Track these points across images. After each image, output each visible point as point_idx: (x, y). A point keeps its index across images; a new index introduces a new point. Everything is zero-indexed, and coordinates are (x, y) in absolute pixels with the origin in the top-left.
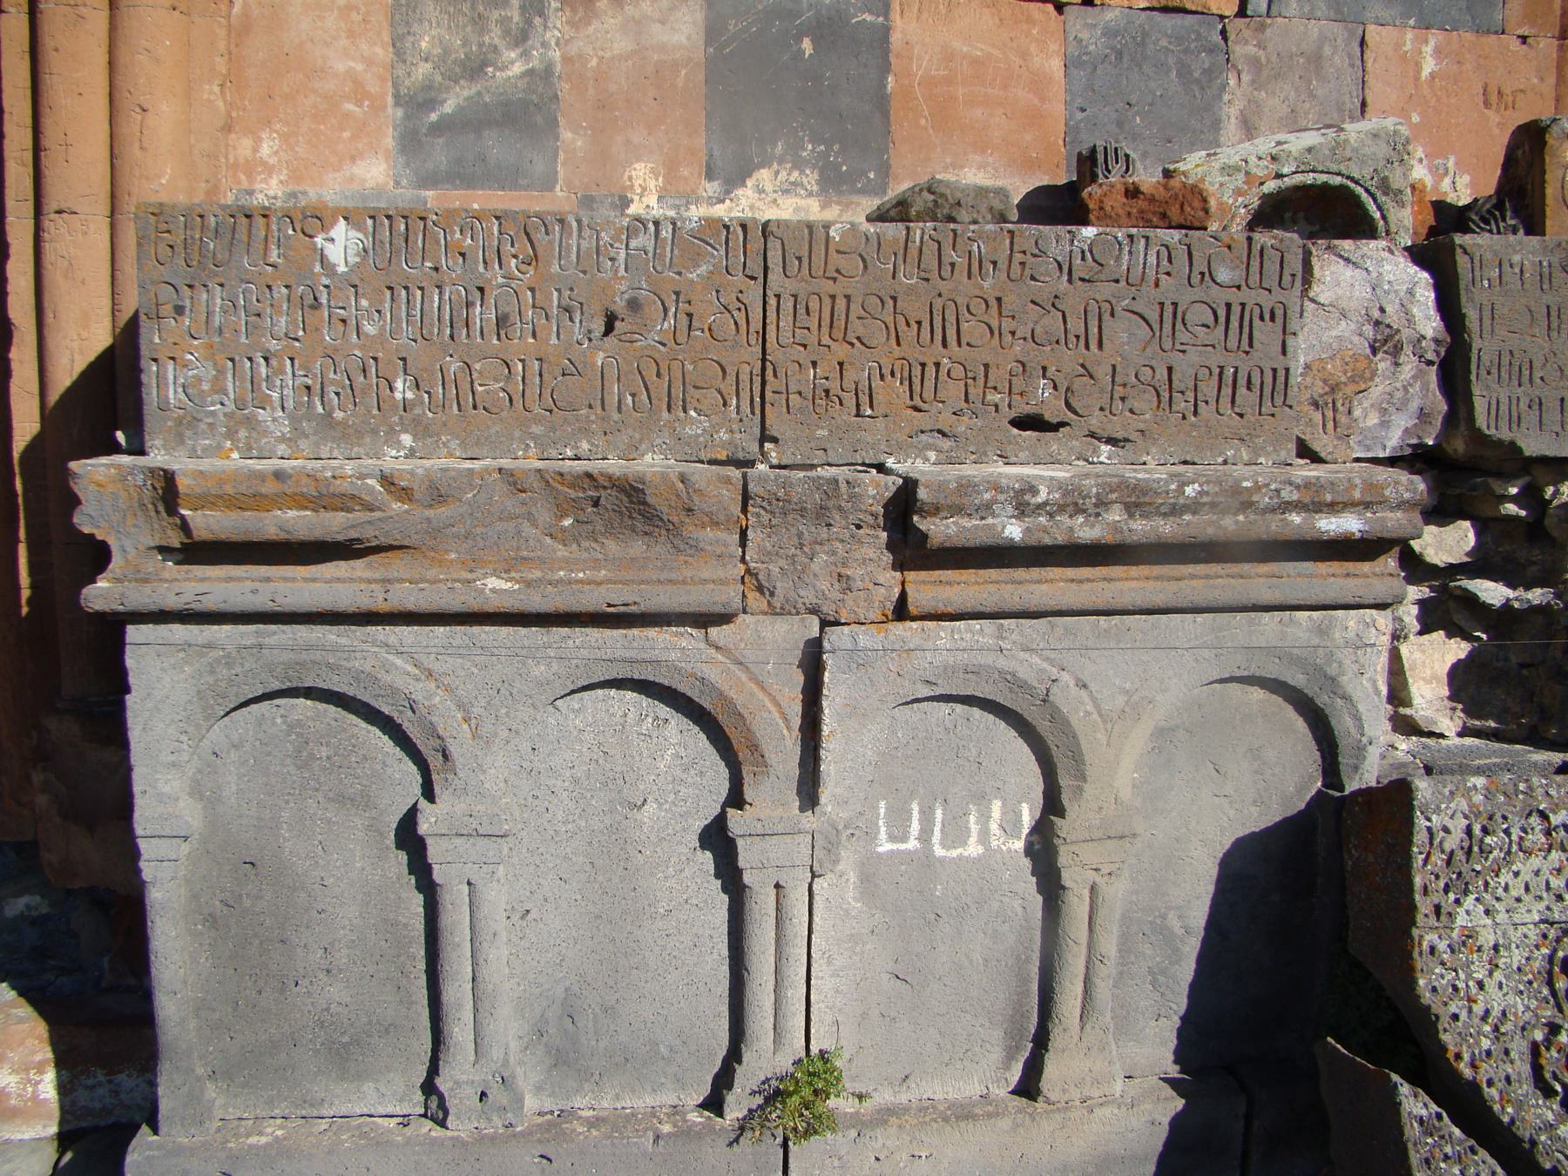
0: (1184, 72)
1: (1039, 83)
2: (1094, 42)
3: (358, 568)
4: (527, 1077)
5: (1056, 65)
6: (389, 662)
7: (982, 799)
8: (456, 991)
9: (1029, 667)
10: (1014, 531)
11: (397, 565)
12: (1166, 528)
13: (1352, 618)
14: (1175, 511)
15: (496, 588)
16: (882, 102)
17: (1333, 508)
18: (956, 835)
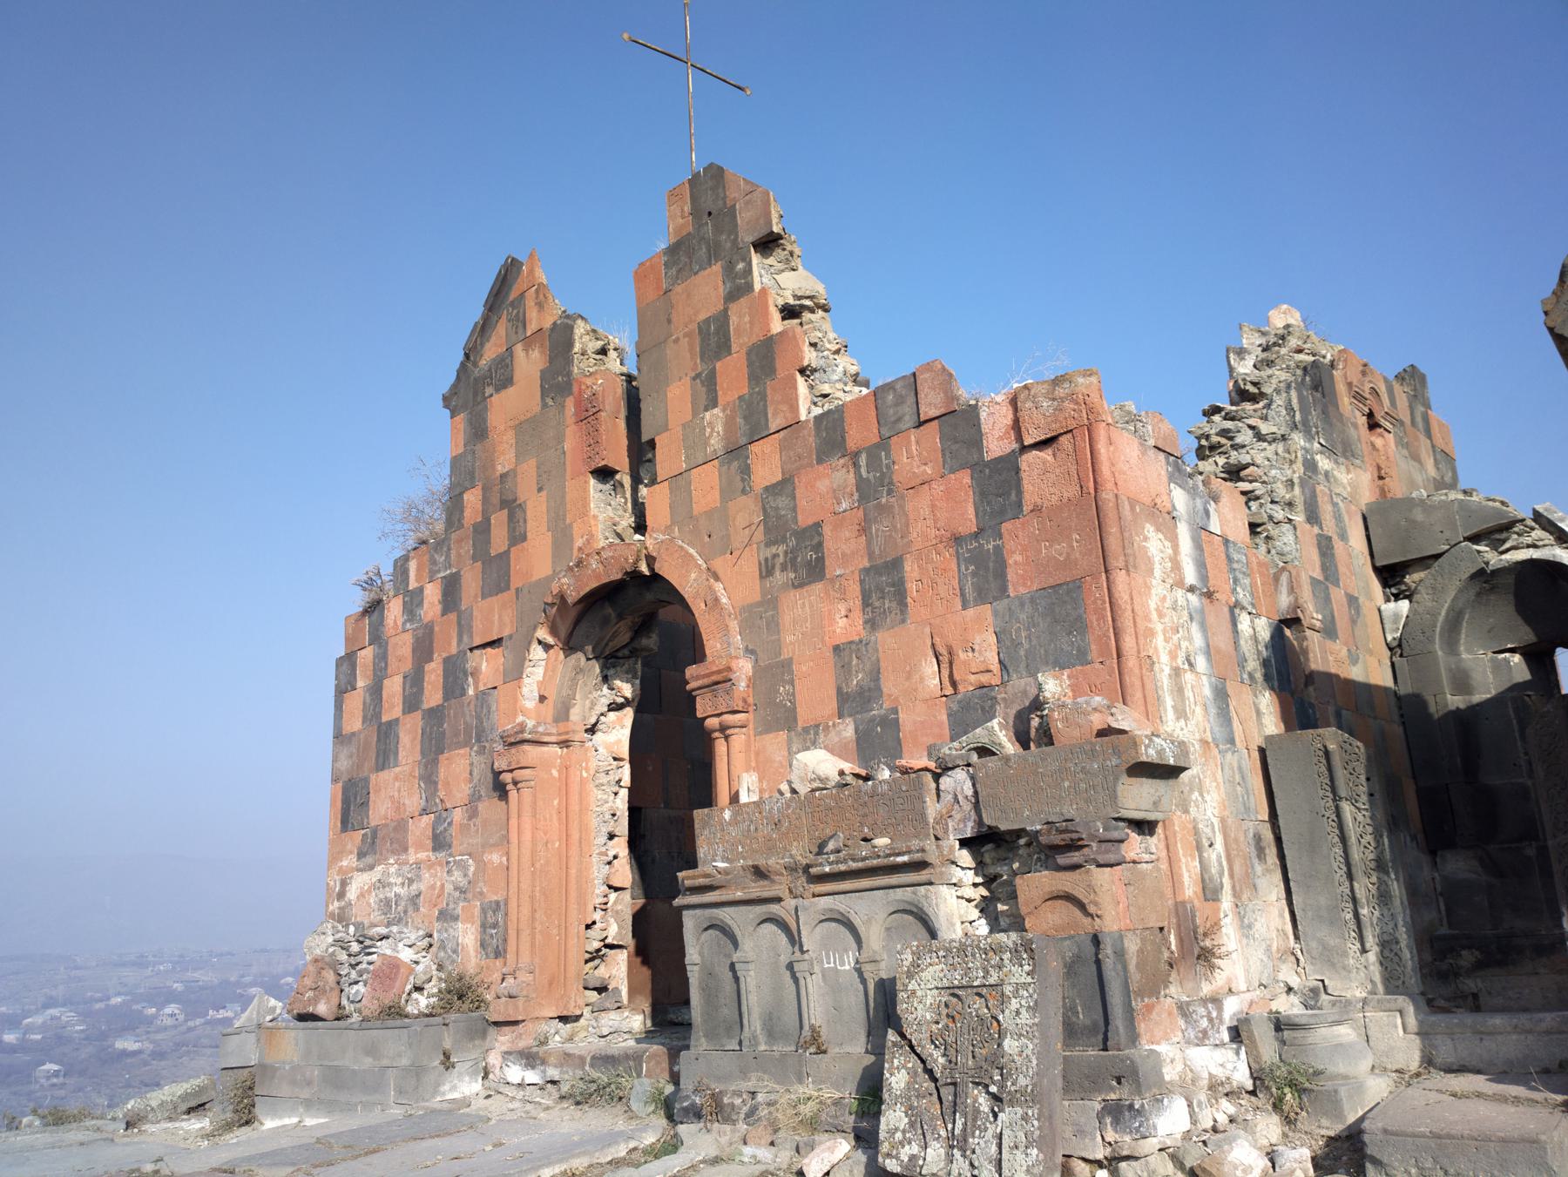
0: (983, 709)
1: (940, 725)
2: (955, 707)
3: (717, 892)
4: (762, 1038)
5: (945, 717)
6: (725, 914)
7: (846, 951)
8: (744, 1008)
9: (842, 908)
10: (827, 869)
11: (723, 891)
12: (860, 865)
13: (922, 888)
14: (863, 859)
15: (739, 895)
16: (899, 741)
17: (899, 854)
18: (843, 964)
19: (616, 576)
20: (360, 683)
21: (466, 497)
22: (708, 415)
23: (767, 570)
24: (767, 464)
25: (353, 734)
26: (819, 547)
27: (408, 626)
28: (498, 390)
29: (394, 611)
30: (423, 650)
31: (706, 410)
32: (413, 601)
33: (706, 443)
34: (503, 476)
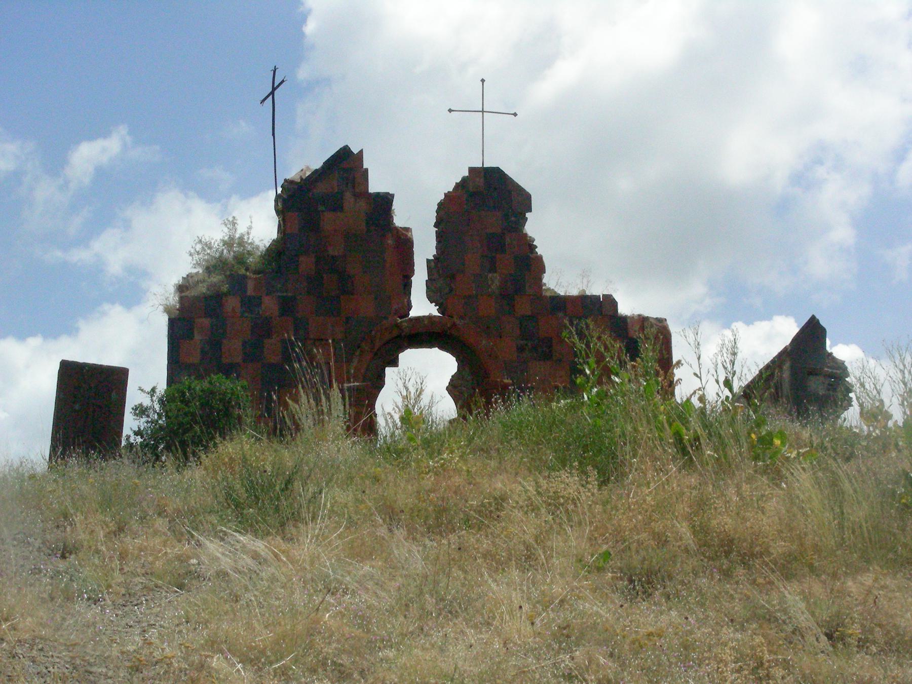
19: (437, 329)
20: (197, 337)
21: (302, 259)
22: (490, 275)
23: (521, 349)
24: (524, 307)
25: (194, 365)
26: (551, 346)
27: (246, 314)
28: (330, 210)
29: (232, 304)
30: (262, 329)
31: (490, 271)
32: (250, 304)
33: (489, 286)
34: (333, 257)
